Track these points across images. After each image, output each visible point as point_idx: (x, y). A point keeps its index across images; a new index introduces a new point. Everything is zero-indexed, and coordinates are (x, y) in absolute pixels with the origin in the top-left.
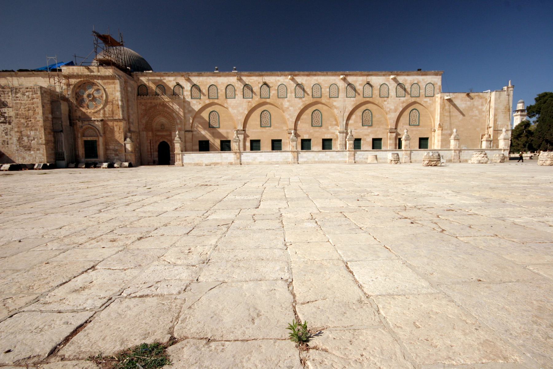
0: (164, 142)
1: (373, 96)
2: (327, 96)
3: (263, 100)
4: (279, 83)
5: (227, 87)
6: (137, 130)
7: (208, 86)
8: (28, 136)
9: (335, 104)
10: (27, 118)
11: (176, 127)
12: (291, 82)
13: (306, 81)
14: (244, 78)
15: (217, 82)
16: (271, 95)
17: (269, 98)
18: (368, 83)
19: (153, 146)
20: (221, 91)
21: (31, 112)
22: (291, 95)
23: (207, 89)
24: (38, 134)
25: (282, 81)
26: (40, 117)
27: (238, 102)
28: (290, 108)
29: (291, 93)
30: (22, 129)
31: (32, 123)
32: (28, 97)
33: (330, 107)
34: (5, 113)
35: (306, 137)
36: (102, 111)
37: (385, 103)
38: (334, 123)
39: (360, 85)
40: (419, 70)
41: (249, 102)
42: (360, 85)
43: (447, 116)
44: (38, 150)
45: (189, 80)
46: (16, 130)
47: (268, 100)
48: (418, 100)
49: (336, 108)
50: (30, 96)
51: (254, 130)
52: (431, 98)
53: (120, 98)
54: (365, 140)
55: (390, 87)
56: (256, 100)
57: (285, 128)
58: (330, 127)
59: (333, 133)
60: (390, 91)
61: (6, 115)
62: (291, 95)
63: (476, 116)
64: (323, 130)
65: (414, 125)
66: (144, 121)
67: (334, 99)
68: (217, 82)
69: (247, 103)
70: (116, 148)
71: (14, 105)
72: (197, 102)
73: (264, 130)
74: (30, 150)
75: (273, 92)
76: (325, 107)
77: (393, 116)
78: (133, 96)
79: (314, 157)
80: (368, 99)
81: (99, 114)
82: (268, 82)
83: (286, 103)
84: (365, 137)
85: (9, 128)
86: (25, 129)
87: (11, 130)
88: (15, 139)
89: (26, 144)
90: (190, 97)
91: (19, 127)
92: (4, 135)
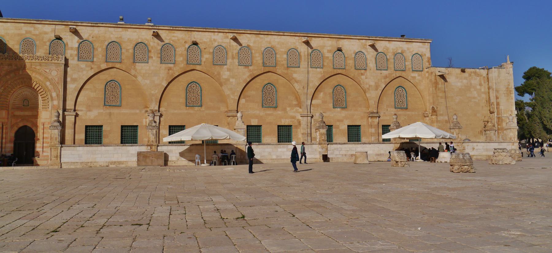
0: (25, 127)
1: (347, 68)
2: (283, 65)
3: (192, 67)
7: (107, 43)
9: (295, 76)
11: (50, 104)
12: (234, 44)
13: (255, 42)
14: (163, 34)
15: (121, 37)
16: (204, 60)
17: (200, 65)
18: (340, 50)
19: (6, 133)
20: (127, 50)
22: (232, 62)
23: (105, 47)
25: (220, 41)
27: (152, 68)
28: (231, 80)
29: (233, 58)
33: (290, 79)
35: (254, 122)
37: (363, 77)
38: (295, 103)
39: (329, 51)
40: (403, 36)
41: (170, 69)
42: (329, 51)
43: (441, 97)
45: (75, 32)
47: (198, 67)
48: (403, 74)
49: (297, 82)
51: (176, 111)
52: (420, 73)
54: (338, 127)
55: (368, 57)
56: (181, 65)
57: (223, 109)
58: (288, 109)
59: (294, 117)
60: (368, 62)
62: (232, 62)
63: (474, 98)
64: (279, 112)
65: (401, 108)
67: (293, 69)
69: (167, 71)
72: (87, 66)
73: (191, 111)
75: (206, 57)
76: (282, 80)
77: (373, 95)
79: (270, 153)
80: (339, 71)
82: (198, 41)
83: (225, 74)
84: (338, 123)
90: (76, 58)
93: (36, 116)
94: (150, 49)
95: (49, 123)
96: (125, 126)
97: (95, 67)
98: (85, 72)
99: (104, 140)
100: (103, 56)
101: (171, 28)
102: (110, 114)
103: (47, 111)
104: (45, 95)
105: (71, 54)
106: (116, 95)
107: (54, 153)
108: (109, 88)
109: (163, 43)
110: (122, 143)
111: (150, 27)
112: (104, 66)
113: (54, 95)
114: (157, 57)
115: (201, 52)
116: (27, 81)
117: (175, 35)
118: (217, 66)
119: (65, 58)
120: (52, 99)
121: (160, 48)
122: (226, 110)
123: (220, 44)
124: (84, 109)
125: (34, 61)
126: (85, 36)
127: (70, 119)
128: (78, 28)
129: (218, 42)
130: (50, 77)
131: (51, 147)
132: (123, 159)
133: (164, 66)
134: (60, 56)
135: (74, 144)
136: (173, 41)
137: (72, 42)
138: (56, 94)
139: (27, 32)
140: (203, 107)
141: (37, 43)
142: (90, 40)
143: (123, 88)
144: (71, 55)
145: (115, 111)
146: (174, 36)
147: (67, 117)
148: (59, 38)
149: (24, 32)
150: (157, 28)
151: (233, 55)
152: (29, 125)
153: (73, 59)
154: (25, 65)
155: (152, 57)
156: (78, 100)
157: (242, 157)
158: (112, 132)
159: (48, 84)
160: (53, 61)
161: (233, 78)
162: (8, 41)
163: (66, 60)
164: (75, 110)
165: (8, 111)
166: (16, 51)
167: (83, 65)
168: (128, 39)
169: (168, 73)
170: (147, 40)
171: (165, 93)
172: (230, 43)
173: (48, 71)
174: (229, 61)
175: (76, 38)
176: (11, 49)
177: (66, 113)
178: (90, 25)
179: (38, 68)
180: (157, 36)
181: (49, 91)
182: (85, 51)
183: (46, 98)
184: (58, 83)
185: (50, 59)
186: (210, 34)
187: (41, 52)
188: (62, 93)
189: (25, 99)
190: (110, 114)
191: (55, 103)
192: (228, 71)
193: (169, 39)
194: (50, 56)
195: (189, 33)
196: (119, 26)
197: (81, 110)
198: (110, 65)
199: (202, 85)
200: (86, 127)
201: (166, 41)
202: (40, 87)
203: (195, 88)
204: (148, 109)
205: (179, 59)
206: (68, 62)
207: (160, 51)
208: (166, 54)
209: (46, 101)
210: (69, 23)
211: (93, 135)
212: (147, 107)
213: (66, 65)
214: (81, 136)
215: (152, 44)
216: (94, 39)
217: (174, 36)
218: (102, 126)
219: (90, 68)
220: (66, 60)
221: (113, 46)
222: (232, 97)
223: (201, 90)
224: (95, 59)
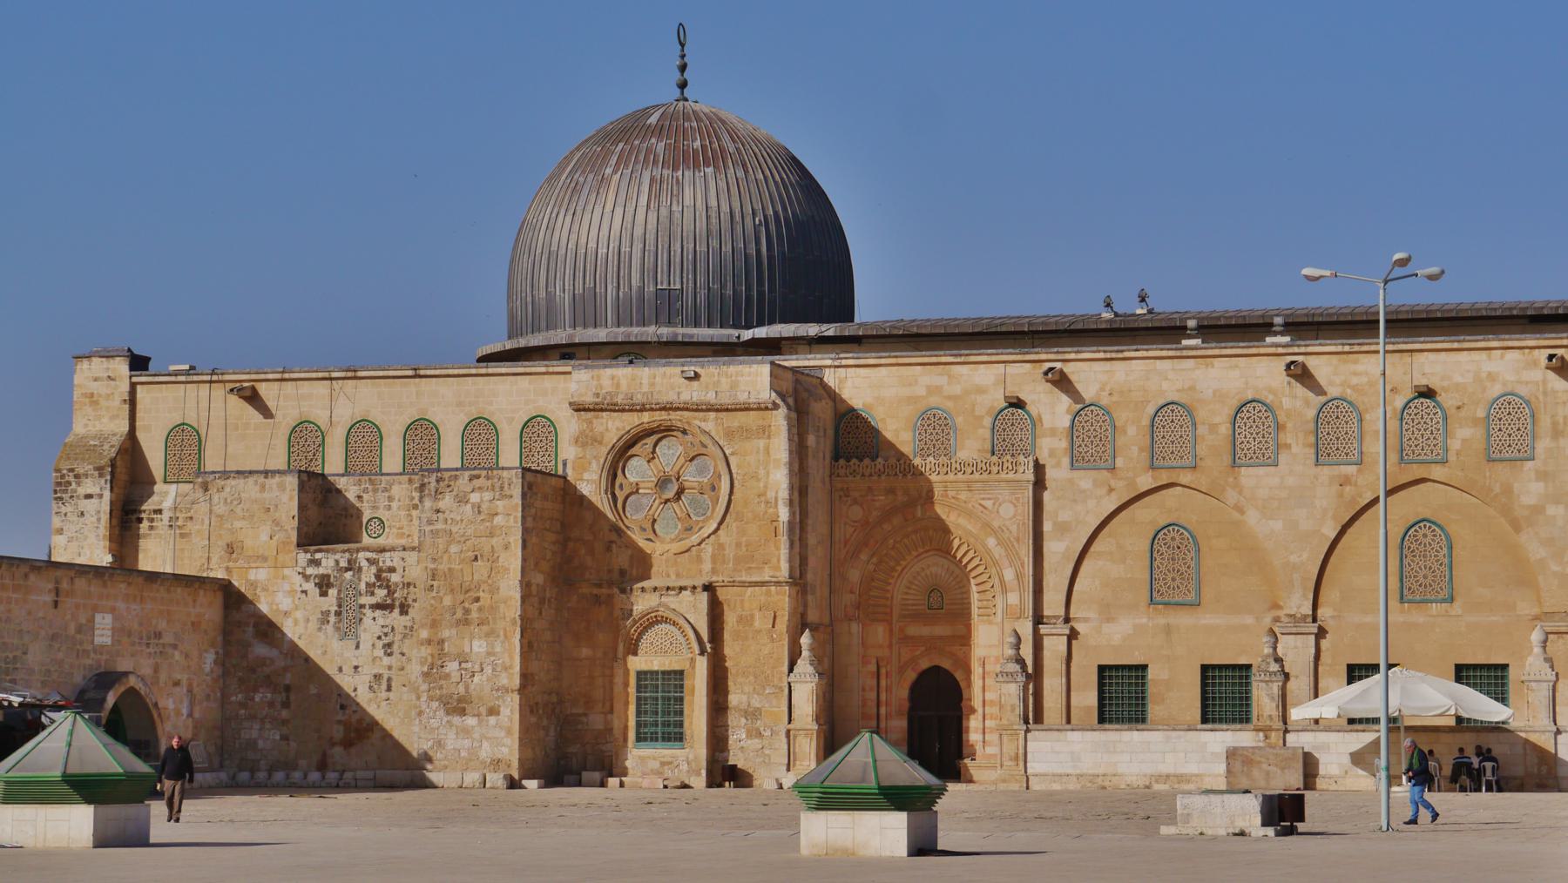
0: (936, 670)
4: (1496, 390)
5: (1239, 410)
6: (826, 620)
7: (1151, 410)
8: (463, 659)
10: (470, 593)
11: (999, 601)
15: (1192, 388)
16: (1455, 444)
17: (1444, 462)
19: (889, 689)
20: (1213, 428)
21: (481, 567)
23: (1146, 422)
24: (498, 649)
25: (1510, 377)
26: (510, 588)
28: (1551, 510)
30: (446, 633)
31: (480, 609)
32: (478, 509)
34: (392, 570)
36: (708, 549)
41: (1345, 481)
44: (493, 711)
45: (1062, 382)
46: (424, 634)
47: (1437, 472)
50: (484, 507)
53: (784, 493)
57: (1526, 608)
61: (395, 578)
66: (854, 575)
68: (1192, 388)
69: (1336, 487)
70: (756, 703)
71: (428, 540)
74: (462, 712)
75: (1464, 436)
78: (818, 468)
81: (699, 559)
82: (1434, 383)
85: (399, 629)
86: (454, 632)
87: (405, 636)
88: (415, 670)
89: (453, 689)
90: (1066, 461)
91: (434, 624)
92: (380, 652)
93: (965, 639)
94: (1282, 418)
95: (997, 659)
96: (1214, 667)
97: (1118, 484)
98: (1091, 503)
99: (1154, 710)
100: (1141, 450)
101: (1347, 348)
102: (1168, 630)
103: (990, 623)
104: (984, 578)
105: (1052, 447)
106: (1183, 569)
107: (1010, 748)
108: (1164, 549)
109: (1323, 399)
110: (1204, 720)
111: (1280, 350)
112: (1145, 482)
113: (1009, 575)
114: (1305, 445)
115: (1445, 418)
116: (938, 537)
117: (1360, 368)
118: (1499, 466)
119: (1036, 462)
120: (1005, 590)
121: (1312, 413)
122: (1536, 611)
123: (1509, 389)
124: (1092, 615)
125: (951, 477)
126: (1088, 392)
127: (1054, 646)
128: (1068, 369)
129: (1504, 384)
130: (996, 524)
131: (1001, 731)
132: (1192, 768)
133: (1326, 471)
134: (1021, 458)
135: (1069, 721)
136: (1354, 388)
137: (1053, 410)
138: (1013, 572)
139: (932, 390)
140: (1457, 604)
141: (959, 420)
142: (1104, 401)
143: (1204, 549)
144: (1052, 453)
145: (1183, 619)
146: (1355, 374)
147: (1047, 642)
148: (1018, 404)
149: (922, 391)
150: (1303, 350)
151: (1555, 424)
152: (946, 664)
153: (1058, 465)
154: (931, 491)
155: (1288, 446)
156: (1076, 587)
157: (1544, 769)
158: (1173, 688)
159: (991, 542)
160: (1003, 476)
161: (1557, 502)
162: (883, 420)
163: (1039, 469)
164: (1067, 620)
165: (890, 623)
166: (906, 449)
167: (1085, 480)
168: (1214, 392)
169: (1341, 495)
170: (1271, 391)
171: (1333, 559)
172: (1545, 382)
173: (988, 504)
174: (1543, 445)
175: (1065, 401)
176: (891, 445)
177: (1043, 629)
178: (1101, 355)
179: (963, 496)
180: (1301, 375)
181: (996, 563)
182: (1091, 437)
183: (987, 586)
184: (1018, 540)
185: (995, 469)
186: (1476, 356)
187: (971, 448)
188: (1029, 570)
189: (934, 590)
190: (1168, 630)
191: (1013, 598)
192: (1538, 479)
193: (1341, 385)
194: (995, 459)
195: (1406, 357)
196: (1185, 353)
197: (1086, 620)
198: (1164, 478)
199: (1453, 529)
200: (1102, 669)
201: (1333, 392)
202: (971, 554)
203: (1428, 540)
204: (1281, 613)
205: (1375, 447)
206: (1044, 474)
207: (1312, 426)
208: (1332, 434)
209: (989, 595)
210: (1043, 357)
211: (1122, 696)
212: (1276, 606)
213: (1039, 484)
214: (1086, 698)
215: (1287, 403)
216: (1114, 399)
217: (1355, 374)
218: (1144, 667)
219: (1105, 490)
220: (1039, 469)
221: (1171, 418)
222: (1555, 568)
223: (1451, 548)
224: (1119, 462)
